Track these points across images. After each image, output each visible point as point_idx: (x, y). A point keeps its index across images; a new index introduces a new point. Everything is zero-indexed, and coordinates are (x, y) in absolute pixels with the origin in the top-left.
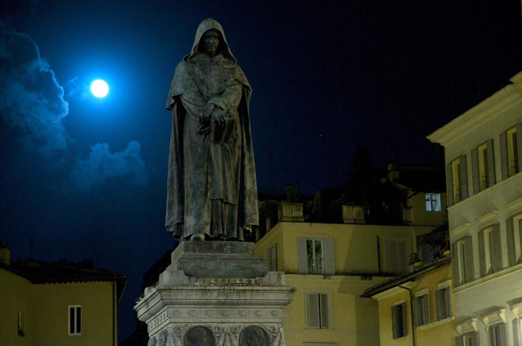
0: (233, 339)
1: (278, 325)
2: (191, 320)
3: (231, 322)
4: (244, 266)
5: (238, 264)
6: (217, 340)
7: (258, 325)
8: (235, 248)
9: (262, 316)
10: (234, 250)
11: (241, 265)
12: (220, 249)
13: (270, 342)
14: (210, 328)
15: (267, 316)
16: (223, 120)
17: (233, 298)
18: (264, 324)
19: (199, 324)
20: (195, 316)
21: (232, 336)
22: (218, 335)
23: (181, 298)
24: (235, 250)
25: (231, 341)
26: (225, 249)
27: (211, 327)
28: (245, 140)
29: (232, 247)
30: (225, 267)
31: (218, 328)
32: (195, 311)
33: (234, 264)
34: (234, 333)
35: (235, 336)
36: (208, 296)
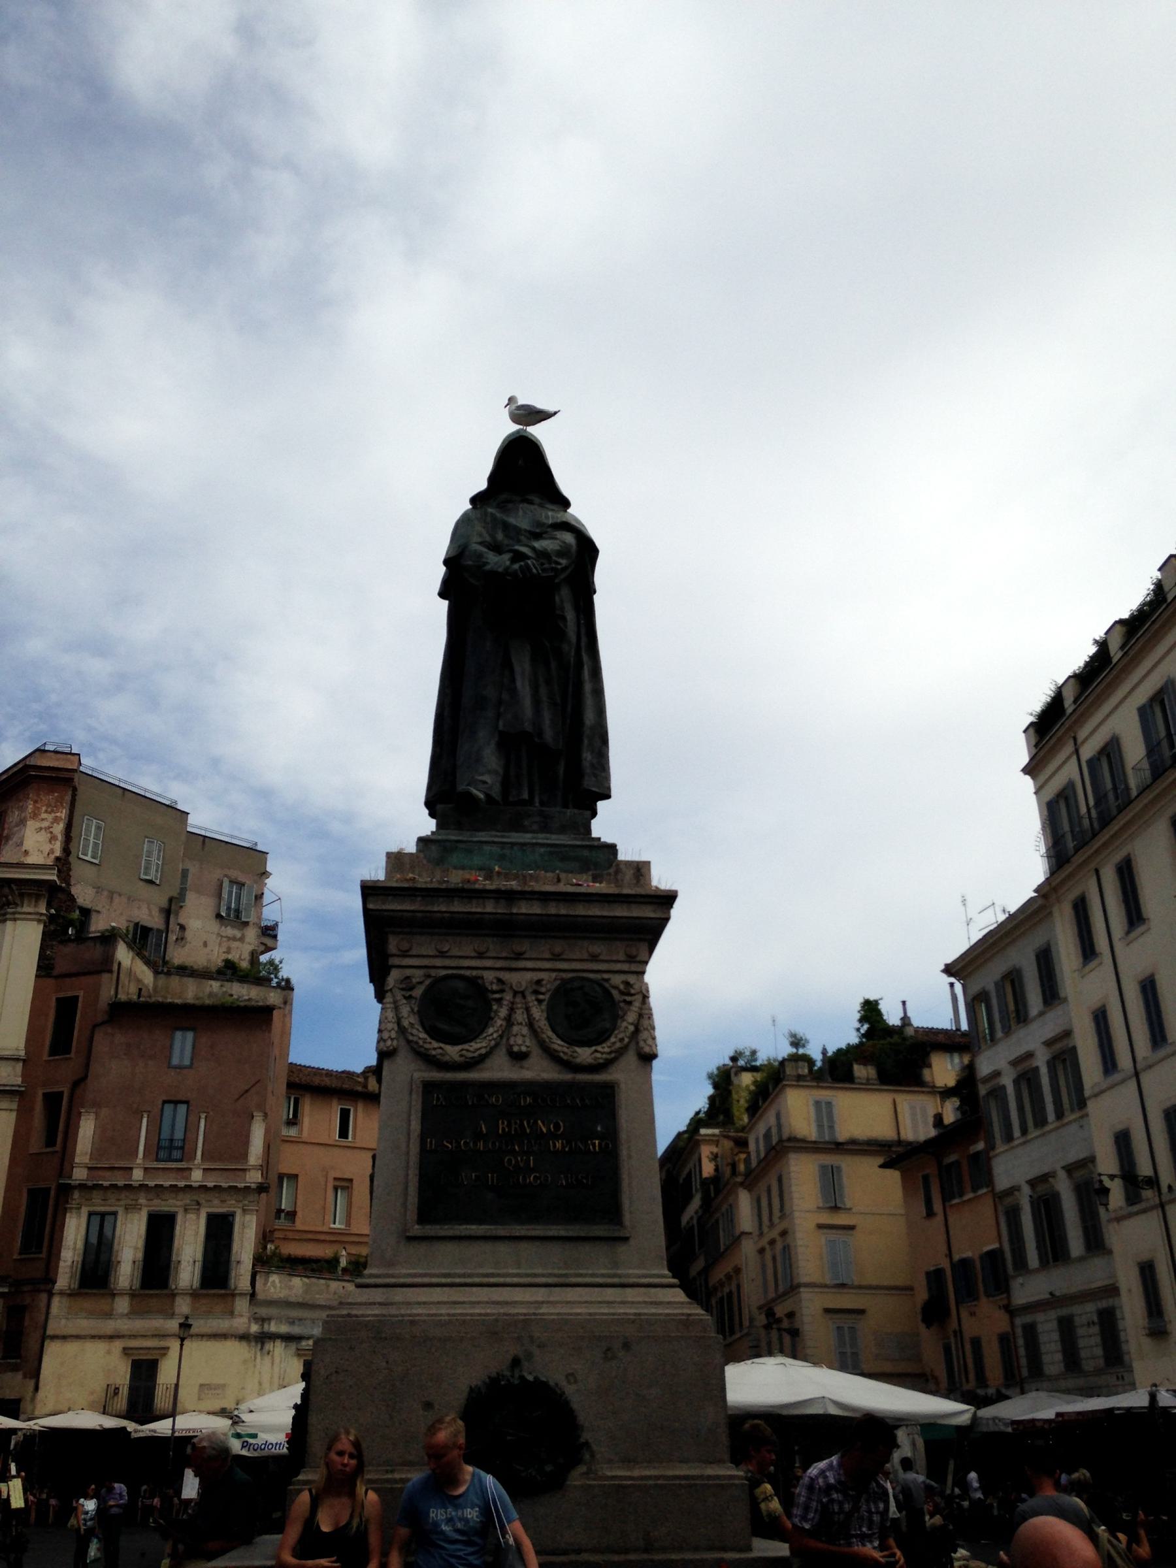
0: (531, 1004)
6: (495, 1007)
7: (591, 976)
12: (517, 826)
14: (480, 981)
18: (606, 976)
19: (454, 972)
20: (446, 952)
21: (531, 998)
22: (497, 996)
23: (412, 908)
27: (482, 978)
28: (584, 640)
31: (500, 981)
33: (542, 850)
34: (536, 992)
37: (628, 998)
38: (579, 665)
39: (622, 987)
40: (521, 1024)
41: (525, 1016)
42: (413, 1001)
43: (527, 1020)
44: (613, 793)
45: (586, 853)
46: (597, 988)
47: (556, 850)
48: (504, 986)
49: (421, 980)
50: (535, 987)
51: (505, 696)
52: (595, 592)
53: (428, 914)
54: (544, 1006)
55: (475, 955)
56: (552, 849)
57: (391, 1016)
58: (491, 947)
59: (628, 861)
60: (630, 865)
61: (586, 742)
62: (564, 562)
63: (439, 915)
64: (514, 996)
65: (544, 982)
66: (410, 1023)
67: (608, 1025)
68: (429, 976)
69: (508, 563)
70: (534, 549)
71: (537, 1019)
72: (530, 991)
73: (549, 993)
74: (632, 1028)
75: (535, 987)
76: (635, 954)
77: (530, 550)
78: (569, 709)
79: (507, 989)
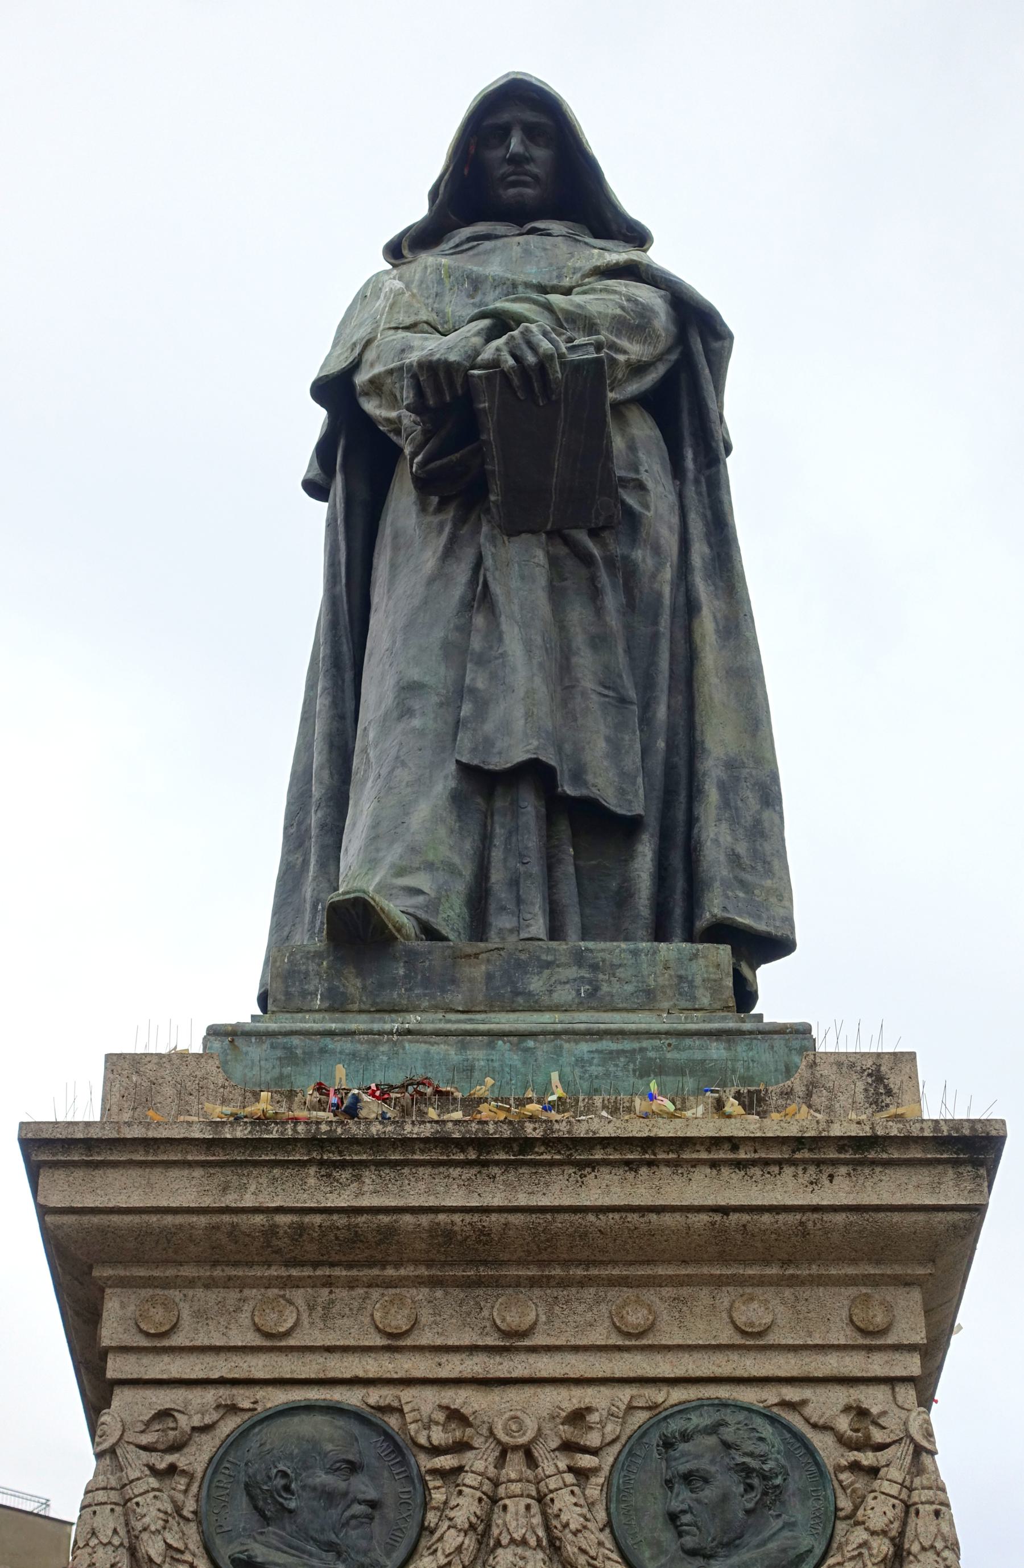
1: (893, 1389)
2: (259, 1367)
3: (544, 1374)
4: (651, 1054)
5: (614, 1046)
6: (438, 1497)
7: (748, 1395)
8: (601, 976)
9: (771, 1339)
10: (596, 989)
11: (633, 1052)
13: (837, 1509)
14: (393, 1421)
15: (810, 1334)
16: (531, 359)
17: (545, 1202)
18: (791, 1394)
20: (287, 1334)
22: (446, 1462)
24: (605, 988)
25: (540, 1499)
26: (536, 984)
27: (400, 1411)
28: (700, 551)
29: (585, 973)
30: (524, 1063)
32: (290, 1302)
33: (584, 1047)
34: (568, 1447)
35: (571, 1469)
36: (365, 1189)
37: (867, 1458)
38: (690, 608)
39: (843, 1424)
40: (524, 1542)
41: (537, 1520)
42: (181, 1482)
43: (541, 1533)
44: (801, 935)
45: (716, 1051)
46: (767, 1430)
47: (627, 1045)
48: (469, 1431)
49: (208, 1420)
50: (566, 1431)
51: (477, 678)
52: (728, 449)
53: (226, 1218)
54: (594, 1489)
55: (379, 1341)
56: (608, 1045)
57: (112, 1525)
58: (426, 1317)
59: (846, 1054)
60: (852, 1066)
61: (712, 795)
62: (635, 350)
63: (259, 1219)
64: (501, 1461)
65: (593, 1418)
66: (169, 1546)
67: (806, 1542)
68: (233, 1409)
69: (477, 341)
70: (548, 308)
71: (573, 1526)
72: (554, 1444)
73: (616, 1448)
74: (882, 1547)
75: (566, 1431)
76: (880, 1319)
77: (534, 307)
78: (661, 712)
79: (477, 1442)
